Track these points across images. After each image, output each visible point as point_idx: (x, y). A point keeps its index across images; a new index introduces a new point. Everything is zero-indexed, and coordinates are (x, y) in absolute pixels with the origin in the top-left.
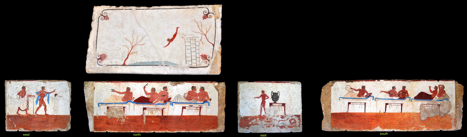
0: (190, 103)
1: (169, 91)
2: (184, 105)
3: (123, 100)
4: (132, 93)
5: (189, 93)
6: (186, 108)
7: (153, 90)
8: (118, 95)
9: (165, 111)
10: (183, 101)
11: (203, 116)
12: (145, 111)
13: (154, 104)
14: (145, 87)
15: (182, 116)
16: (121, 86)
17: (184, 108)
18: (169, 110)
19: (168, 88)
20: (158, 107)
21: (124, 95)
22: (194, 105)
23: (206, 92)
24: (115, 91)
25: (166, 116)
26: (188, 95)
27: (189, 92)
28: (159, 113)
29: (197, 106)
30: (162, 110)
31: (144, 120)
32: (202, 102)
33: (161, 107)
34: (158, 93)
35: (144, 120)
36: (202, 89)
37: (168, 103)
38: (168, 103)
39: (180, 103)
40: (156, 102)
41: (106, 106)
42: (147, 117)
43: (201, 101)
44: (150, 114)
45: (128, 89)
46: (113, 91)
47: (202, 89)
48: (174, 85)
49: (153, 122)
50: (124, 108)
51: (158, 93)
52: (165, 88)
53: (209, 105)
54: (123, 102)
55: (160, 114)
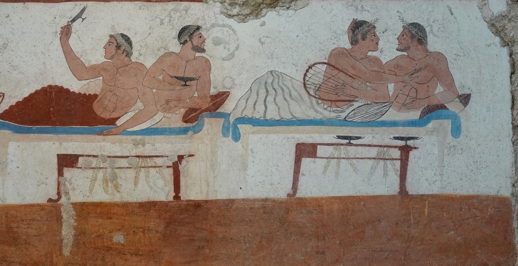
0: (345, 122)
1: (213, 52)
2: (308, 136)
5: (335, 62)
6: (321, 151)
7: (120, 45)
9: (191, 170)
10: (301, 111)
11: (423, 198)
12: (68, 172)
13: (123, 131)
15: (294, 203)
17: (305, 151)
19: (209, 36)
20: (147, 150)
22: (369, 136)
23: (440, 57)
25: (197, 205)
26: (327, 78)
27: (338, 53)
28: (155, 188)
29: (385, 136)
31: (67, 232)
32: (415, 115)
33: (167, 147)
34: (149, 62)
35: (67, 232)
36: (415, 35)
37: (207, 120)
38: (207, 120)
40: (135, 120)
42: (83, 210)
43: (405, 106)
44: (100, 195)
47: (415, 35)
48: (243, 18)
49: (119, 238)
51: (149, 62)
52: (188, 34)
53: (456, 131)
55: (163, 193)
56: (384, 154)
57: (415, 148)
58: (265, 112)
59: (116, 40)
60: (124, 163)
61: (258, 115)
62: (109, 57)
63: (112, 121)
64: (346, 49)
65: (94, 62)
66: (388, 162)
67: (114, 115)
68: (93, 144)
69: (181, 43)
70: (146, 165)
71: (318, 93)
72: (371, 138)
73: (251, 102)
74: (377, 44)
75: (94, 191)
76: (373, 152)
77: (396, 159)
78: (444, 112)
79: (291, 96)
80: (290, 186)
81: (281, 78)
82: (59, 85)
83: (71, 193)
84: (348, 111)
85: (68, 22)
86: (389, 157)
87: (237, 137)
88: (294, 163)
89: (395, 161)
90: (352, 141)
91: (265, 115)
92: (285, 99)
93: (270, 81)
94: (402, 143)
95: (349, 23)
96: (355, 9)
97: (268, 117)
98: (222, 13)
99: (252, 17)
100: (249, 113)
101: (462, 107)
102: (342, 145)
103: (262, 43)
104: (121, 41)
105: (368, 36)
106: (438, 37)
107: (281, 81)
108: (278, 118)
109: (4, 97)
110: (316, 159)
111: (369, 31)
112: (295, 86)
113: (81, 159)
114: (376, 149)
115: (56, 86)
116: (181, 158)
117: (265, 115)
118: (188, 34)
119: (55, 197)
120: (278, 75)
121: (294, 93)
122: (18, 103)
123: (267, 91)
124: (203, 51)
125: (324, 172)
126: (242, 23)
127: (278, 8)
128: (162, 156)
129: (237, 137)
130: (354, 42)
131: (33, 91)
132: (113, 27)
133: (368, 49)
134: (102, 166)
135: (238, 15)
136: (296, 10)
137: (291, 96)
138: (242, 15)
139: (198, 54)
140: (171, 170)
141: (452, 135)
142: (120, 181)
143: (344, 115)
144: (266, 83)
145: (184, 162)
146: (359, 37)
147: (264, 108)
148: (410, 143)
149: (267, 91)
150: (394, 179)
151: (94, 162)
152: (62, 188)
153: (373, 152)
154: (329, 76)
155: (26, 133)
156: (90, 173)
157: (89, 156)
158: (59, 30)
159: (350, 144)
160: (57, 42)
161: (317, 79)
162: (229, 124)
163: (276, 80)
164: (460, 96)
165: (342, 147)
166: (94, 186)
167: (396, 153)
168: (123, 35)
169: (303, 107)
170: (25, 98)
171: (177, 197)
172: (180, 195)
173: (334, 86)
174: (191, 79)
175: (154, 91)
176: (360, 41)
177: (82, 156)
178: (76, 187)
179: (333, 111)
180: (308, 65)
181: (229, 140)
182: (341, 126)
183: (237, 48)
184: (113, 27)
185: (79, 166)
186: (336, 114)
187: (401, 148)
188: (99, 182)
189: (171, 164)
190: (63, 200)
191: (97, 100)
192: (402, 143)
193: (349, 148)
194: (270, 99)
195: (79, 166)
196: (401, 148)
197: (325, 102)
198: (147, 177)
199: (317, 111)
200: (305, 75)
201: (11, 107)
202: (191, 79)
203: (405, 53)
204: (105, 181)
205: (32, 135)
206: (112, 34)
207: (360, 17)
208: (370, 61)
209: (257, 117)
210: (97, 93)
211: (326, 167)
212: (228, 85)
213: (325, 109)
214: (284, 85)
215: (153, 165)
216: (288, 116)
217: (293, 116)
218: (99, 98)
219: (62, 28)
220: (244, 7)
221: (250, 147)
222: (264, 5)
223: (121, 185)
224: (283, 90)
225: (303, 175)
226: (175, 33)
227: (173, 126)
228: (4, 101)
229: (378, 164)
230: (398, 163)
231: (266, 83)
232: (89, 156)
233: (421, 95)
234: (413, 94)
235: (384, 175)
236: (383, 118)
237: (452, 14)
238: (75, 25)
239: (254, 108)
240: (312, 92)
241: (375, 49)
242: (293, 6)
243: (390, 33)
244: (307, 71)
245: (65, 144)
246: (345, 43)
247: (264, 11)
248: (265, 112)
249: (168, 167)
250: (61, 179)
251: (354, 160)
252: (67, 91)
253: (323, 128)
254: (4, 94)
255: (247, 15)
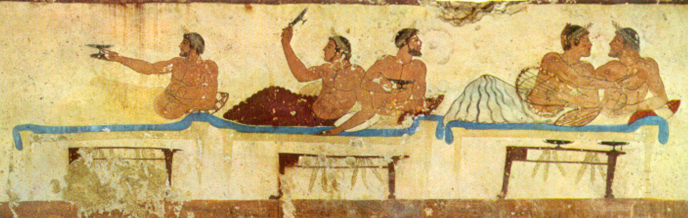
0: (555, 127)
3: (162, 110)
4: (213, 68)
6: (530, 154)
8: (132, 77)
13: (341, 132)
14: (287, 34)
15: (505, 204)
16: (149, 26)
17: (515, 154)
18: (427, 165)
21: (164, 81)
24: (113, 57)
30: (391, 168)
32: (624, 120)
33: (384, 148)
36: (626, 40)
39: (493, 126)
40: (353, 121)
41: (62, 147)
43: (616, 112)
44: (318, 194)
45: (192, 44)
46: (102, 53)
47: (626, 40)
50: (169, 154)
52: (405, 37)
53: (664, 137)
54: (161, 120)
56: (592, 158)
57: (624, 153)
58: (478, 115)
59: (335, 43)
60: (342, 163)
61: (471, 117)
62: (329, 59)
63: (330, 122)
64: (559, 55)
65: (313, 64)
66: (596, 166)
67: (332, 117)
68: (313, 144)
69: (398, 47)
70: (363, 165)
71: (530, 98)
72: (579, 143)
73: (464, 106)
74: (589, 49)
75: (313, 188)
76: (581, 156)
77: (603, 164)
78: (654, 118)
79: (503, 100)
80: (500, 188)
81: (494, 83)
82: (281, 86)
83: (292, 191)
84: (558, 116)
85: (290, 24)
86: (597, 162)
87: (449, 140)
88: (504, 165)
89: (602, 166)
90: (561, 146)
91: (477, 119)
92: (498, 103)
93: (483, 85)
94: (609, 148)
95: (562, 28)
96: (569, 13)
97: (481, 120)
98: (440, 17)
99: (467, 21)
100: (462, 116)
101: (669, 112)
102: (552, 149)
103: (477, 48)
104: (340, 44)
105: (581, 42)
106: (651, 43)
107: (494, 86)
108: (490, 122)
109: (228, 97)
110: (527, 163)
111: (582, 36)
112: (508, 91)
113: (300, 158)
114: (585, 153)
115: (278, 88)
116: (396, 159)
117: (477, 119)
118: (405, 37)
119: (276, 194)
120: (491, 80)
121: (506, 96)
122: (242, 104)
123: (480, 95)
124: (420, 54)
125: (534, 175)
126: (458, 28)
127: (493, 12)
128: (378, 157)
129: (449, 140)
130: (567, 47)
131: (255, 91)
132: (333, 30)
133: (580, 54)
134: (321, 165)
135: (453, 19)
136: (511, 15)
137: (503, 100)
138: (457, 19)
139: (414, 58)
140: (386, 171)
141: (660, 141)
142: (338, 181)
143: (554, 120)
144: (479, 87)
145: (400, 162)
146: (572, 42)
147: (476, 112)
148: (618, 148)
149: (480, 95)
150: (601, 182)
151: (313, 161)
152: (284, 186)
153: (581, 156)
154: (541, 81)
155: (249, 132)
156: (308, 172)
157: (309, 155)
158: (281, 32)
159: (558, 148)
160: (279, 43)
161: (530, 84)
162: (443, 125)
163: (489, 85)
164: (670, 102)
165: (551, 151)
166: (313, 184)
167: (604, 158)
168: (343, 40)
169: (515, 111)
170: (249, 100)
171: (392, 196)
172: (395, 194)
173: (546, 90)
174: (407, 83)
175: (371, 93)
176: (573, 47)
177: (302, 155)
178: (296, 184)
179: (544, 116)
180: (521, 69)
181: (443, 141)
182: (551, 130)
183: (452, 52)
184: (333, 30)
185: (299, 164)
186: (547, 119)
187: (608, 153)
188: (319, 179)
189: (386, 165)
190: (285, 197)
191: (316, 102)
192: (609, 148)
193: (559, 153)
194: (483, 103)
195: (299, 164)
196: (608, 153)
197: (536, 106)
198: (363, 176)
199: (527, 115)
200: (518, 80)
201: (236, 107)
202: (407, 83)
203: (617, 59)
204: (324, 180)
205: (255, 135)
206: (332, 36)
207: (573, 23)
208: (582, 66)
209: (470, 120)
210: (317, 95)
211: (535, 170)
212: (443, 89)
213: (537, 114)
214: (498, 90)
215: (370, 165)
216: (499, 120)
217: (504, 119)
218: (318, 100)
219: (283, 30)
220: (460, 12)
221: (462, 150)
222: (479, 10)
223: (339, 184)
224: (495, 94)
225: (513, 177)
226: (392, 35)
227: (387, 127)
228: (228, 101)
229: (585, 168)
230: (606, 168)
231: (479, 87)
232: (309, 155)
233: (632, 99)
234: (622, 101)
235: (591, 178)
236: (594, 123)
237: (666, 19)
238: (296, 27)
239: (467, 111)
240: (523, 97)
241: (588, 54)
242: (508, 11)
243: (601, 38)
244: (520, 76)
245: (286, 143)
246: (557, 47)
247: (479, 15)
248: (478, 115)
249: (384, 167)
250: (283, 177)
251: (563, 164)
252: (289, 92)
253: (533, 132)
254: (228, 95)
255: (463, 19)
